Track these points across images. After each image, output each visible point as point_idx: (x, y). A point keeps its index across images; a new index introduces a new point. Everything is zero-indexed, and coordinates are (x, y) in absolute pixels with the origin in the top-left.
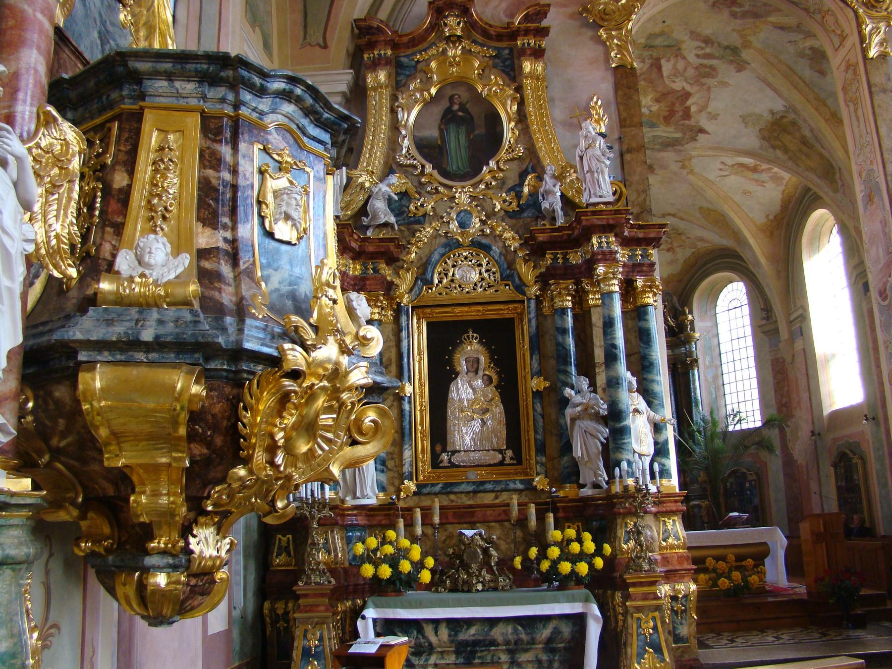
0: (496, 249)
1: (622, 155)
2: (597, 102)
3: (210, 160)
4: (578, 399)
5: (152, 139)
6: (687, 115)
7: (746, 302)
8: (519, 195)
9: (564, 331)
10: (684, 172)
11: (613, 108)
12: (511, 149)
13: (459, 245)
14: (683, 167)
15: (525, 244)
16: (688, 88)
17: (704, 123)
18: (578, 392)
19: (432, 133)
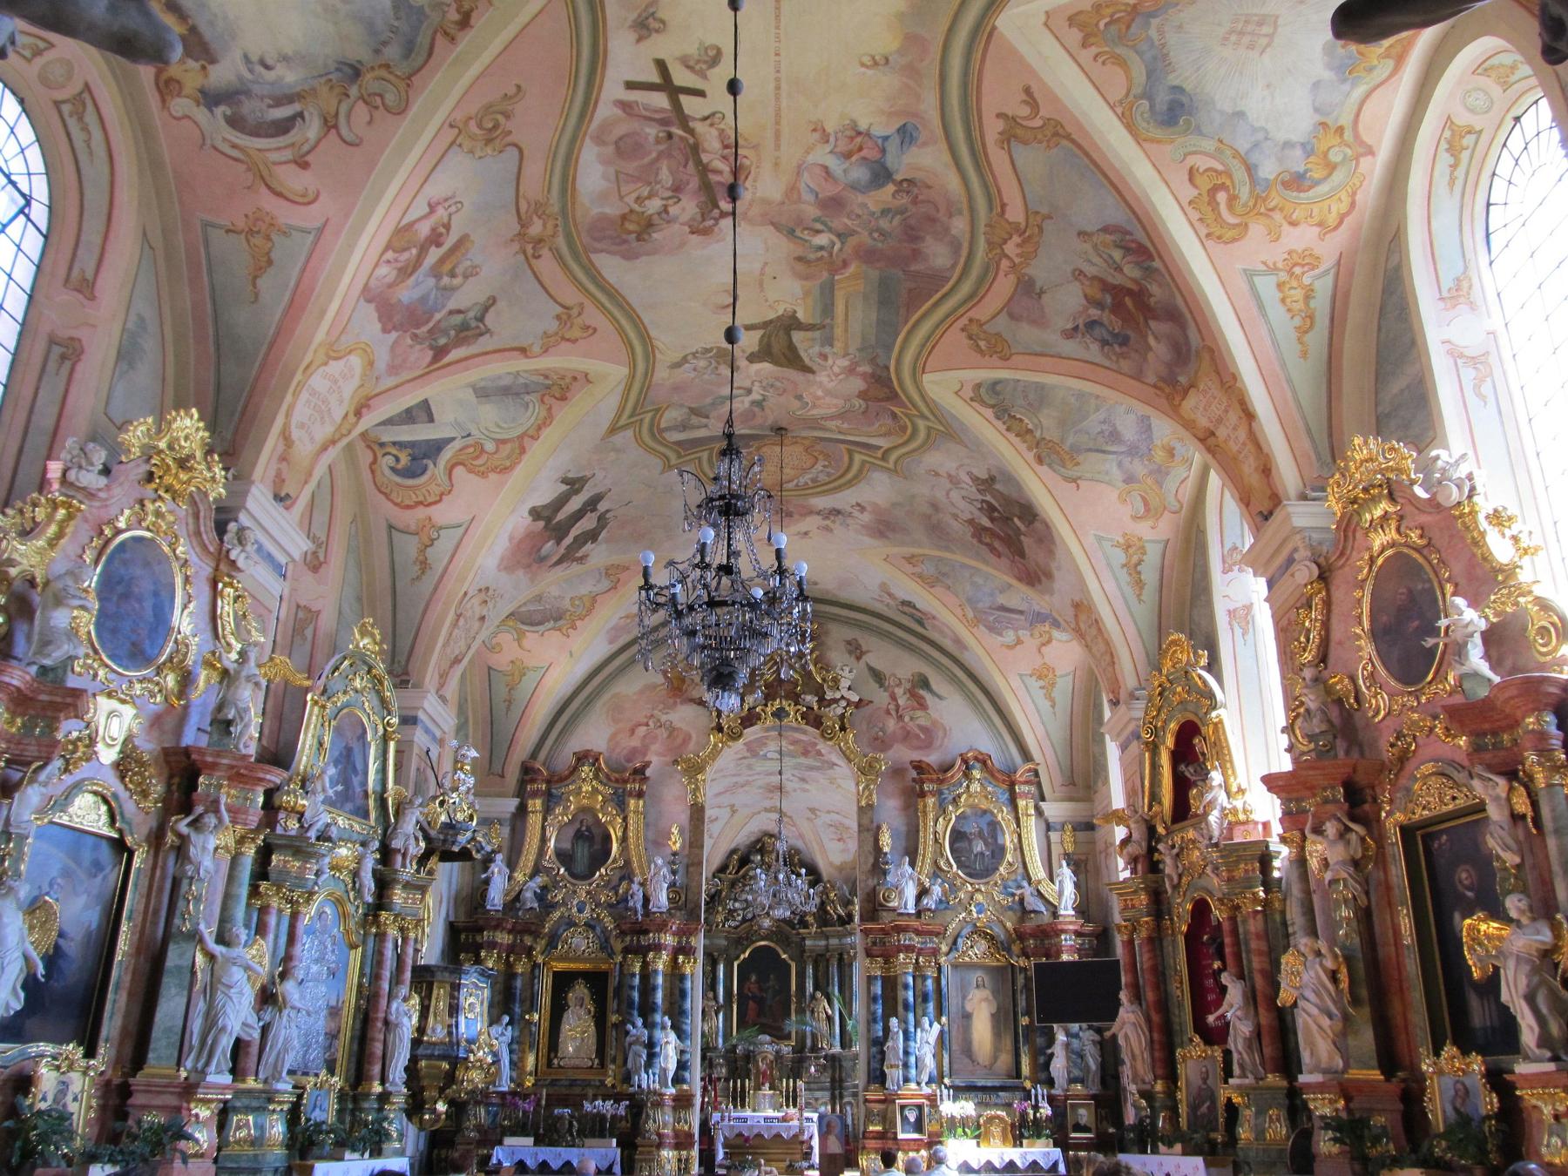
0: (598, 930)
1: (688, 866)
2: (675, 830)
3: (452, 997)
4: (634, 1031)
5: (435, 992)
8: (616, 893)
9: (632, 988)
11: (687, 836)
12: (615, 861)
13: (575, 925)
15: (617, 927)
18: (634, 1026)
19: (567, 845)
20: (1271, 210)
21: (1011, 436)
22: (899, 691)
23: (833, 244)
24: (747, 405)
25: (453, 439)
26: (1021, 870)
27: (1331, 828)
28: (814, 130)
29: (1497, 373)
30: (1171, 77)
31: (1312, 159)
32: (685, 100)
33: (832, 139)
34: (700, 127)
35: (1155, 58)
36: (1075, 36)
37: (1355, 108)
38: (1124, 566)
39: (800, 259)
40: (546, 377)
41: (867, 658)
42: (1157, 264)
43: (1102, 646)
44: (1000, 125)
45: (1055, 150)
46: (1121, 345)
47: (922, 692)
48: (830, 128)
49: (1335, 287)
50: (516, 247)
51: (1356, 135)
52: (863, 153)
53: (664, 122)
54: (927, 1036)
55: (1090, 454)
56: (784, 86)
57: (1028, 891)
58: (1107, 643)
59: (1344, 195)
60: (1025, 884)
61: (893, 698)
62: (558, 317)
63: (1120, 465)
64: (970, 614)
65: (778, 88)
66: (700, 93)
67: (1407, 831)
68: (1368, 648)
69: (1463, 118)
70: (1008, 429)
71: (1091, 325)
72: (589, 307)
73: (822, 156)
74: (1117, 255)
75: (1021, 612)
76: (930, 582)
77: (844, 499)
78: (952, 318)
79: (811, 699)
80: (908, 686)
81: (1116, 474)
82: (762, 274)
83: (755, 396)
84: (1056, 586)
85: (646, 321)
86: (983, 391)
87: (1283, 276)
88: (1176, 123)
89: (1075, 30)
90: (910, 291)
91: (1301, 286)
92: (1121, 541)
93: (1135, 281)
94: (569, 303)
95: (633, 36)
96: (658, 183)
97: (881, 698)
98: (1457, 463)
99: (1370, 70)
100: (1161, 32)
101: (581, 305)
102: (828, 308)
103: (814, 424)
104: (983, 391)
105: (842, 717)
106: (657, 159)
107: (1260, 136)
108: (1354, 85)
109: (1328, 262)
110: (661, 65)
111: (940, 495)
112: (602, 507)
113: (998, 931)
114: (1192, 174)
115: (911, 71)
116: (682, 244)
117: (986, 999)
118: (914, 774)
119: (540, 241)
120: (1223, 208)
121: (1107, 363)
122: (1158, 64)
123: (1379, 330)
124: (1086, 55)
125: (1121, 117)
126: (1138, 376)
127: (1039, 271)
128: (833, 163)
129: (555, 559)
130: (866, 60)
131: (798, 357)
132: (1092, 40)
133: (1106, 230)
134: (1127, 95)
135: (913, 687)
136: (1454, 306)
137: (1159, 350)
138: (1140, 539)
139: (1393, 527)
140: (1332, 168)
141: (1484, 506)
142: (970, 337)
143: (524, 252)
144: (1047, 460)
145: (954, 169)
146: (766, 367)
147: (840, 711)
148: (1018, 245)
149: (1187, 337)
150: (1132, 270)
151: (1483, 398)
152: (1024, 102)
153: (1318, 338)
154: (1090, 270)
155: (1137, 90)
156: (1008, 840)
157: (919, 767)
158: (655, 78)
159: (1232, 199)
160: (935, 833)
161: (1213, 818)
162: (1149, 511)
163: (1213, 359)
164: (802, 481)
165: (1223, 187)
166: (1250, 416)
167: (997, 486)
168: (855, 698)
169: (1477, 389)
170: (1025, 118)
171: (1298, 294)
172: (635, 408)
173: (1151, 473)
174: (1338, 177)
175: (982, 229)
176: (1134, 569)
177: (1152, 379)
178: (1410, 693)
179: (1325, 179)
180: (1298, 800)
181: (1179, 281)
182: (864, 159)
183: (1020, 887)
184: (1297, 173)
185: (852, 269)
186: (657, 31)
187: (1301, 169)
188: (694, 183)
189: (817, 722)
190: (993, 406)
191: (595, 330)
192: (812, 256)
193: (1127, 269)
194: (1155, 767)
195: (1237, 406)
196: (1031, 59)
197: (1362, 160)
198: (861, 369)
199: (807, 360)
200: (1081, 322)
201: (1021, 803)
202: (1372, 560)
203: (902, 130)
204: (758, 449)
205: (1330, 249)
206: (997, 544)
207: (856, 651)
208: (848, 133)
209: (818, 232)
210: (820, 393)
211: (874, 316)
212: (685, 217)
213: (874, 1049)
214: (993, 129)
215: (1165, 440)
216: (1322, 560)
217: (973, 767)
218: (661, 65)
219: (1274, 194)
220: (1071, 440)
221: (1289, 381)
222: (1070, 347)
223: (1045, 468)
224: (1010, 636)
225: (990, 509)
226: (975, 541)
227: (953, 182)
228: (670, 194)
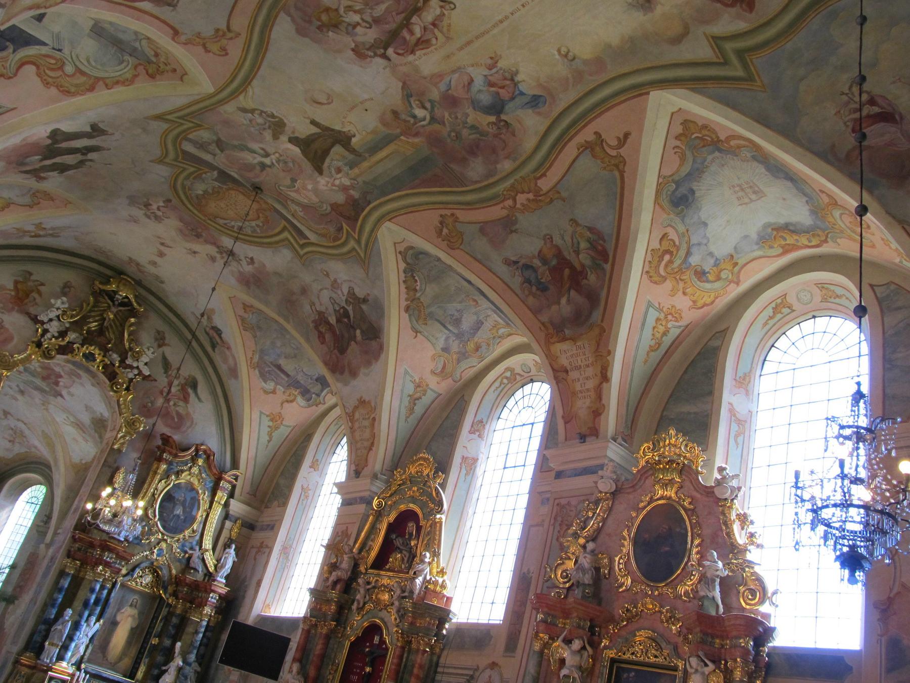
6: (57, 383)
7: (40, 503)
10: (43, 407)
14: (43, 405)
16: (62, 374)
17: (64, 393)
20: (681, 280)
21: (403, 286)
22: (176, 382)
23: (424, 119)
24: (256, 161)
25: (44, 44)
26: (197, 538)
27: (577, 644)
28: (491, 58)
29: (747, 434)
30: (695, 183)
31: (715, 268)
33: (494, 70)
35: (698, 169)
36: (679, 129)
37: (751, 258)
38: (409, 396)
39: (395, 113)
40: (157, 55)
41: (167, 351)
42: (608, 267)
43: (367, 434)
44: (591, 138)
46: (538, 289)
47: (190, 391)
48: (499, 65)
49: (678, 337)
51: (739, 272)
52: (501, 91)
54: (90, 629)
55: (436, 323)
56: (505, 24)
57: (197, 553)
58: (373, 436)
59: (713, 295)
60: (197, 548)
61: (170, 385)
62: (217, 30)
63: (447, 339)
64: (256, 359)
65: (501, 22)
67: (613, 661)
68: (628, 547)
69: (792, 299)
70: (404, 282)
71: (527, 267)
73: (478, 76)
74: (583, 245)
75: (288, 375)
76: (245, 325)
77: (242, 249)
78: (441, 206)
79: (116, 357)
80: (183, 381)
81: (441, 343)
82: (362, 103)
83: (267, 161)
84: (354, 383)
85: (260, 73)
86: (411, 252)
87: (662, 316)
91: (666, 327)
92: (417, 381)
93: (583, 266)
96: (372, 8)
97: (162, 381)
98: (733, 477)
99: (771, 247)
101: (238, 35)
102: (374, 148)
103: (284, 200)
104: (411, 252)
105: (131, 380)
107: (705, 241)
108: (759, 249)
109: (683, 323)
111: (316, 287)
112: (91, 156)
113: (164, 573)
114: (664, 236)
115: (579, 76)
116: (339, 51)
117: (133, 616)
118: (160, 443)
120: (664, 263)
121: (519, 292)
122: (696, 173)
123: (685, 372)
124: (673, 142)
125: (658, 184)
126: (536, 312)
127: (524, 221)
128: (479, 82)
129: (28, 168)
131: (323, 162)
132: (683, 138)
133: (590, 229)
135: (186, 384)
136: (739, 388)
137: (564, 307)
138: (427, 385)
139: (674, 490)
140: (718, 278)
141: (738, 507)
142: (441, 223)
144: (411, 312)
145: (538, 138)
146: (296, 150)
147: (131, 376)
149: (591, 313)
150: (585, 258)
151: (737, 444)
153: (656, 356)
154: (557, 241)
155: (676, 178)
156: (200, 515)
157: (166, 440)
159: (671, 262)
160: (156, 489)
161: (419, 581)
162: (443, 373)
163: (601, 335)
164: (233, 223)
165: (671, 253)
166: (605, 377)
167: (364, 307)
168: (147, 373)
169: (736, 437)
170: (610, 146)
171: (661, 329)
172: (188, 114)
173: (459, 353)
174: (717, 285)
175: (517, 176)
176: (414, 400)
177: (545, 318)
178: (648, 586)
179: (712, 282)
180: (554, 616)
181: (613, 284)
182: (498, 93)
183: (192, 549)
184: (704, 270)
185: (416, 140)
187: (707, 270)
188: (392, 26)
189: (112, 376)
190: (408, 264)
191: (227, 54)
194: (373, 529)
195: (599, 368)
196: (647, 124)
197: (732, 284)
198: (352, 192)
199: (326, 165)
200: (523, 261)
201: (219, 494)
202: (651, 500)
204: (228, 190)
205: (690, 316)
206: (328, 336)
207: (160, 341)
208: (507, 74)
209: (424, 107)
210: (310, 187)
212: (360, 39)
213: (42, 627)
214: (587, 135)
215: (480, 340)
216: (620, 484)
217: (200, 457)
219: (688, 273)
220: (433, 309)
221: (632, 371)
222: (502, 270)
223: (407, 315)
224: (270, 386)
225: (343, 315)
226: (312, 325)
227: (529, 144)
228: (369, 19)
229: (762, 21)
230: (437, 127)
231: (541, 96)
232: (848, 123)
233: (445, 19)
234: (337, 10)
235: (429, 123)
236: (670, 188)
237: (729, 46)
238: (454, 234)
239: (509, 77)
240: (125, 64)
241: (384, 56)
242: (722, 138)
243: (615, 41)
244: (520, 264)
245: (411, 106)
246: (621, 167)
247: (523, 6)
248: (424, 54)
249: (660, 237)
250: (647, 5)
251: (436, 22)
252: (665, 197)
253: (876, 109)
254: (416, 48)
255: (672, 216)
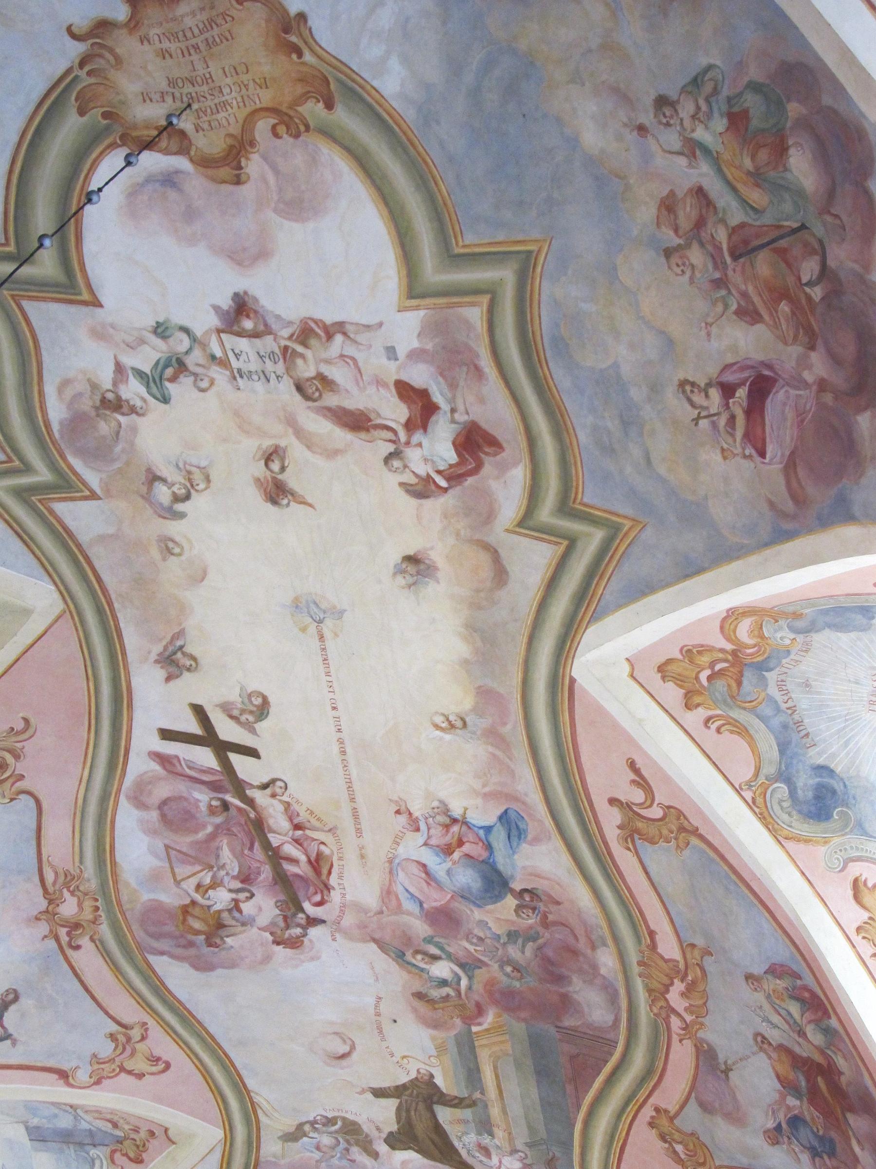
28: (398, 812)
30: (812, 752)
32: (234, 758)
34: (260, 798)
35: (785, 727)
36: (673, 694)
40: (115, 1125)
42: (834, 1022)
45: (687, 853)
48: (416, 814)
50: (43, 928)
53: (215, 787)
56: (349, 750)
62: (112, 1037)
66: (253, 753)
71: (795, 1121)
72: (156, 1031)
74: (794, 1008)
78: (631, 1109)
82: (378, 1014)
88: (828, 817)
89: (670, 685)
90: (573, 1058)
94: (126, 1020)
95: (160, 673)
100: (781, 686)
102: (473, 1075)
106: (212, 837)
110: (199, 711)
115: (493, 736)
116: (267, 959)
119: (77, 926)
125: (752, 805)
128: (430, 858)
130: (439, 720)
132: (697, 699)
134: (757, 775)
142: (663, 1138)
143: (57, 939)
146: (410, 1155)
148: (683, 994)
150: (816, 1037)
152: (633, 782)
154: (775, 1036)
155: (769, 769)
158: (193, 727)
170: (639, 805)
175: (636, 969)
182: (467, 856)
185: (490, 1018)
186: (189, 670)
188: (267, 873)
192: (435, 993)
193: (809, 1030)
196: (626, 723)
200: (781, 1117)
203: (504, 818)
208: (441, 819)
209: (435, 958)
211: (534, 1093)
212: (264, 920)
218: (199, 711)
229: (524, 444)
230: (481, 975)
231: (506, 812)
232: (747, 452)
233: (295, 807)
234: (194, 903)
235: (470, 978)
236: (778, 795)
237: (545, 514)
238: (691, 1147)
239: (448, 821)
240: (97, 1163)
241: (313, 922)
242: (729, 647)
243: (462, 649)
244: (784, 1125)
245: (422, 970)
246: (686, 823)
247: (334, 708)
248: (340, 877)
249: (850, 893)
250: (422, 567)
251: (296, 821)
252: (785, 817)
253: (742, 393)
254: (324, 877)
255: (836, 840)
